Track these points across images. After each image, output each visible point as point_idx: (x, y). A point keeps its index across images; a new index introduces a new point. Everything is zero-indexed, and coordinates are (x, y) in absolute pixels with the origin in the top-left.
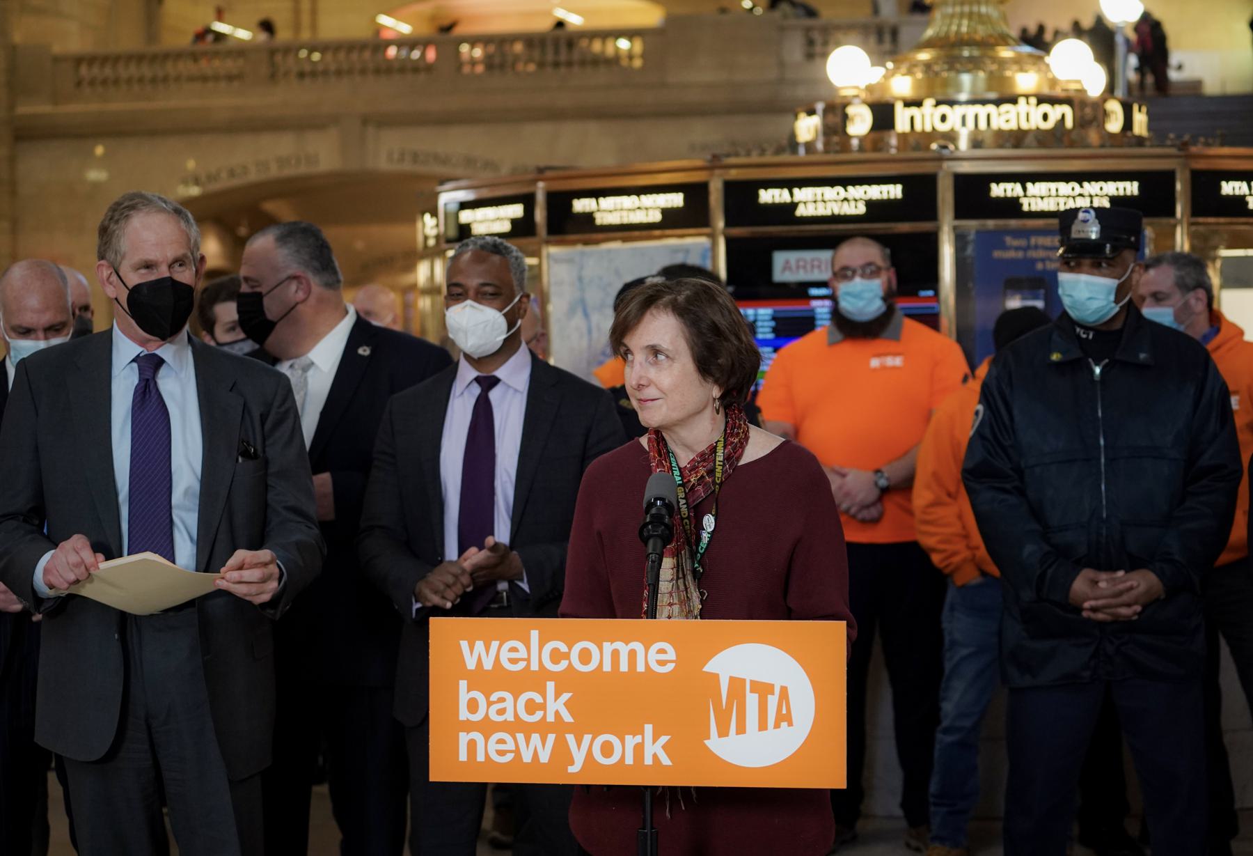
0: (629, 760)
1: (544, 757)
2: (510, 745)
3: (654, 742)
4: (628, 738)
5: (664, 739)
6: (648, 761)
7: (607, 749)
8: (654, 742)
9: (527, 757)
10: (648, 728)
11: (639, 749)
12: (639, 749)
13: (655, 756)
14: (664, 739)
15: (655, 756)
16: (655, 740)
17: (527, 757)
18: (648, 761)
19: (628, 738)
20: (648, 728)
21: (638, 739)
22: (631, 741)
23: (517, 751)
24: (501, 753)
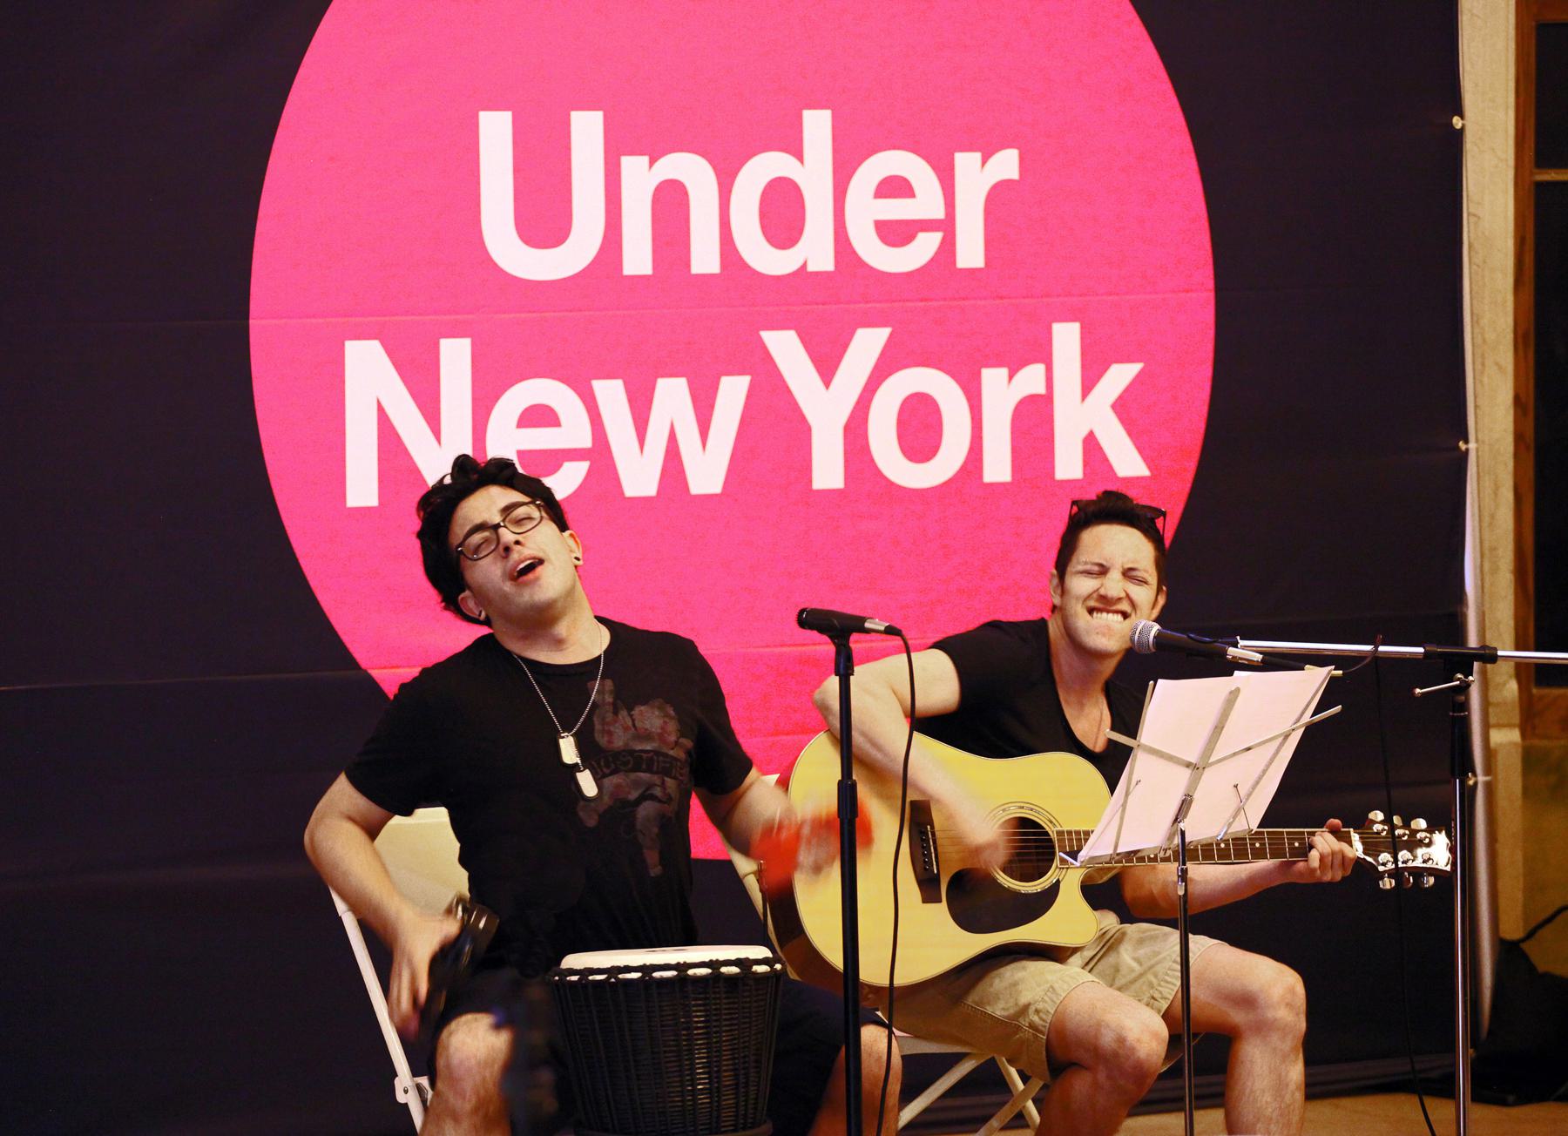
0: (998, 468)
1: (707, 473)
2: (574, 431)
3: (1087, 387)
4: (992, 378)
5: (1120, 376)
6: (1068, 465)
8: (1087, 387)
10: (1067, 338)
11: (1034, 420)
12: (1034, 420)
13: (1091, 445)
14: (1120, 376)
15: (1091, 445)
17: (639, 476)
18: (1068, 465)
19: (992, 378)
20: (1067, 338)
21: (1031, 379)
22: (1003, 391)
23: (599, 454)
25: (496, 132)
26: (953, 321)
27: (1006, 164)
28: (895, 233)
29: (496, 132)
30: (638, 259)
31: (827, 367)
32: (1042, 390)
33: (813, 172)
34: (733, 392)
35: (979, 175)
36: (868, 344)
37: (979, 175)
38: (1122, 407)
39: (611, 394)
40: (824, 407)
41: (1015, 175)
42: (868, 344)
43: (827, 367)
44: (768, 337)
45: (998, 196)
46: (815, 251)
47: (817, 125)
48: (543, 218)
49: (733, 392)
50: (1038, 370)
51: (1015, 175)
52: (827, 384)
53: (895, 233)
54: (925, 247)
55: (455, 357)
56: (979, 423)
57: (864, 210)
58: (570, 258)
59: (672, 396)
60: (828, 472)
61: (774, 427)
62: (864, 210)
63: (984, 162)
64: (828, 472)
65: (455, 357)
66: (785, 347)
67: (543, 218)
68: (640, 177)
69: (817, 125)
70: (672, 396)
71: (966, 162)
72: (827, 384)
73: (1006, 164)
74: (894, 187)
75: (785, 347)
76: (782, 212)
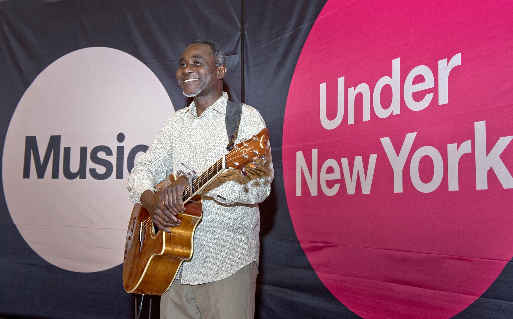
3: (489, 148)
4: (451, 147)
5: (504, 142)
6: (482, 184)
7: (426, 169)
8: (489, 148)
10: (480, 127)
14: (504, 142)
16: (490, 146)
18: (482, 184)
19: (451, 147)
20: (480, 127)
21: (466, 147)
22: (455, 152)
23: (342, 181)
25: (323, 87)
26: (441, 126)
27: (457, 60)
29: (323, 87)
31: (398, 150)
32: (470, 151)
34: (373, 158)
35: (445, 67)
36: (410, 138)
37: (445, 67)
38: (505, 157)
40: (397, 163)
41: (459, 63)
42: (410, 138)
43: (398, 150)
44: (382, 140)
45: (454, 73)
49: (373, 158)
50: (469, 143)
51: (459, 63)
52: (398, 156)
53: (418, 96)
54: (429, 98)
57: (410, 88)
61: (384, 169)
62: (410, 88)
63: (448, 61)
66: (386, 142)
68: (352, 93)
71: (442, 64)
72: (398, 156)
73: (457, 60)
74: (419, 79)
75: (386, 142)
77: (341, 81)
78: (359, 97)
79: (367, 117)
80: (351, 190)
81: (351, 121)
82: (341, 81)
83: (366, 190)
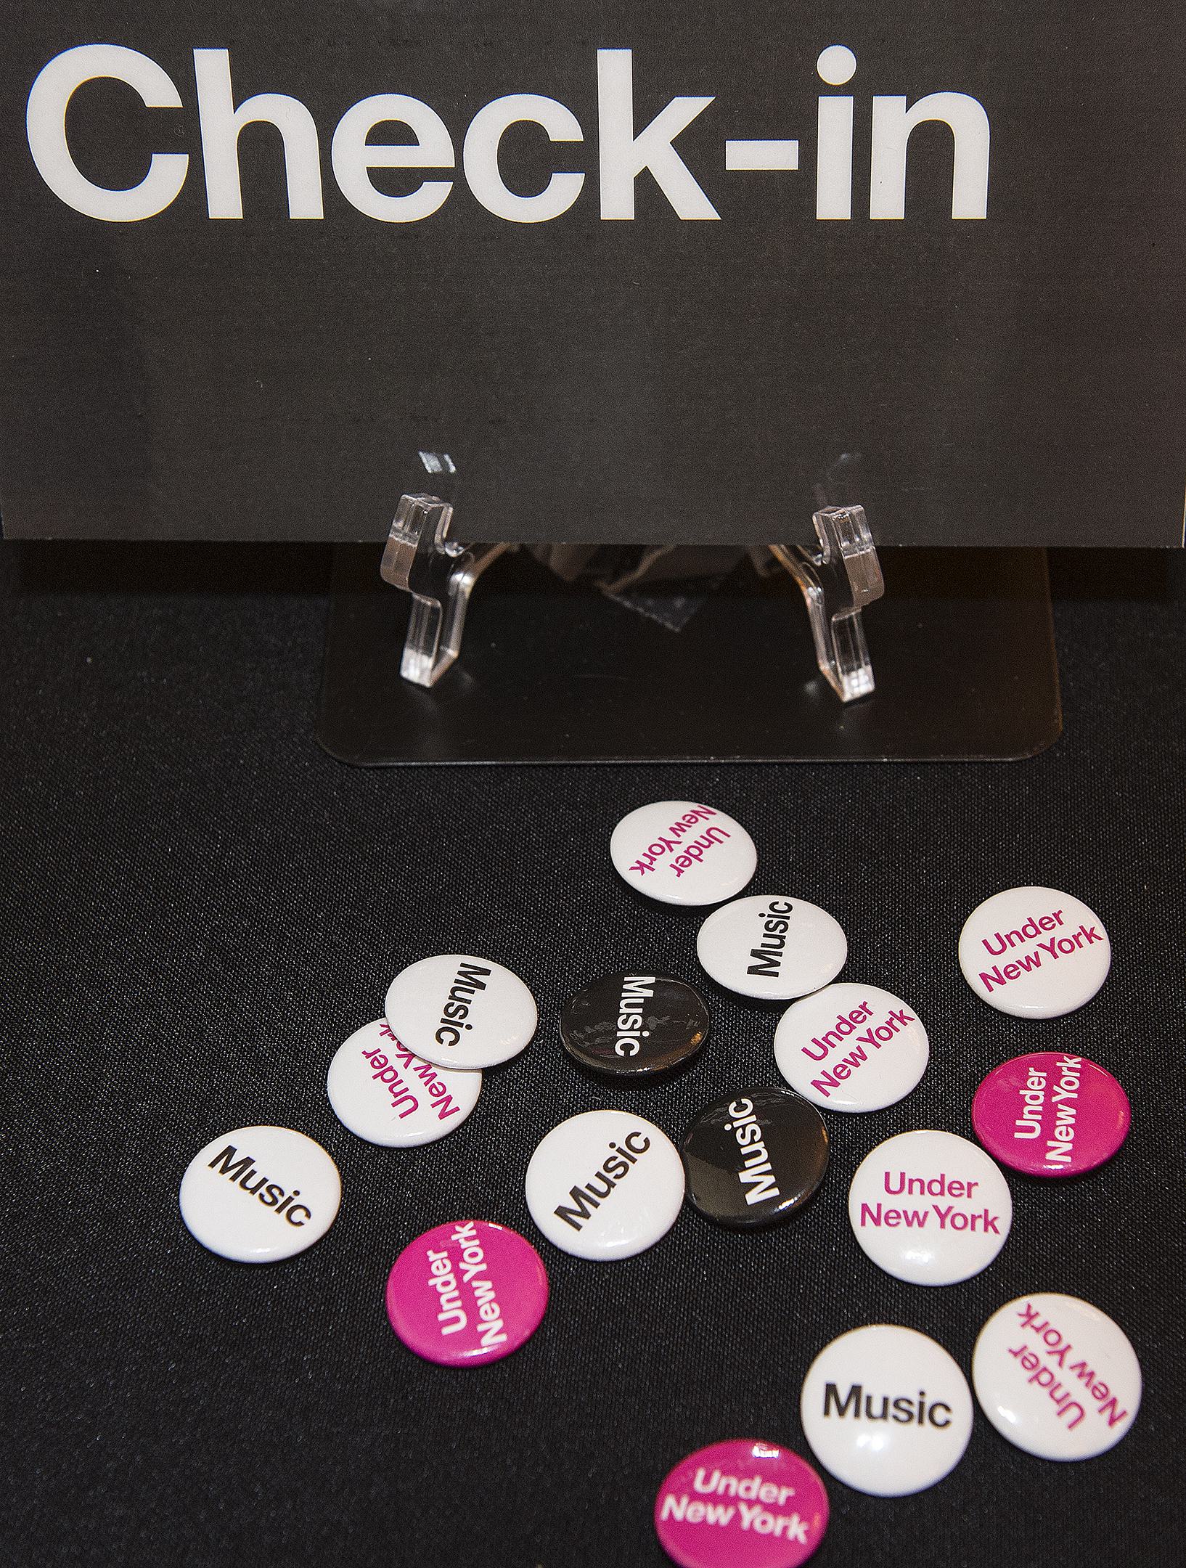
9: (1072, 1121)
10: (1059, 1064)
20: (1059, 1064)
22: (1065, 1072)
24: (1068, 1134)
25: (1017, 1135)
28: (1040, 1083)
29: (1017, 1135)
30: (1039, 1117)
33: (1029, 1093)
34: (1060, 1106)
36: (1056, 1088)
39: (1058, 1123)
40: (1065, 1095)
42: (1056, 1088)
46: (1041, 1094)
47: (1022, 1092)
48: (1031, 1130)
49: (1060, 1106)
53: (1040, 1083)
55: (1050, 1143)
56: (1069, 1076)
58: (1038, 1127)
59: (1059, 1115)
60: (1075, 1096)
64: (1075, 1096)
65: (1050, 1143)
66: (1055, 1099)
67: (1031, 1130)
68: (1027, 1116)
69: (1022, 1092)
70: (1059, 1115)
75: (1055, 1099)
76: (1035, 1098)
77: (1019, 1123)
78: (1031, 1112)
79: (1040, 1108)
80: (1072, 1121)
81: (1039, 1117)
82: (1019, 1123)
83: (1073, 1112)
